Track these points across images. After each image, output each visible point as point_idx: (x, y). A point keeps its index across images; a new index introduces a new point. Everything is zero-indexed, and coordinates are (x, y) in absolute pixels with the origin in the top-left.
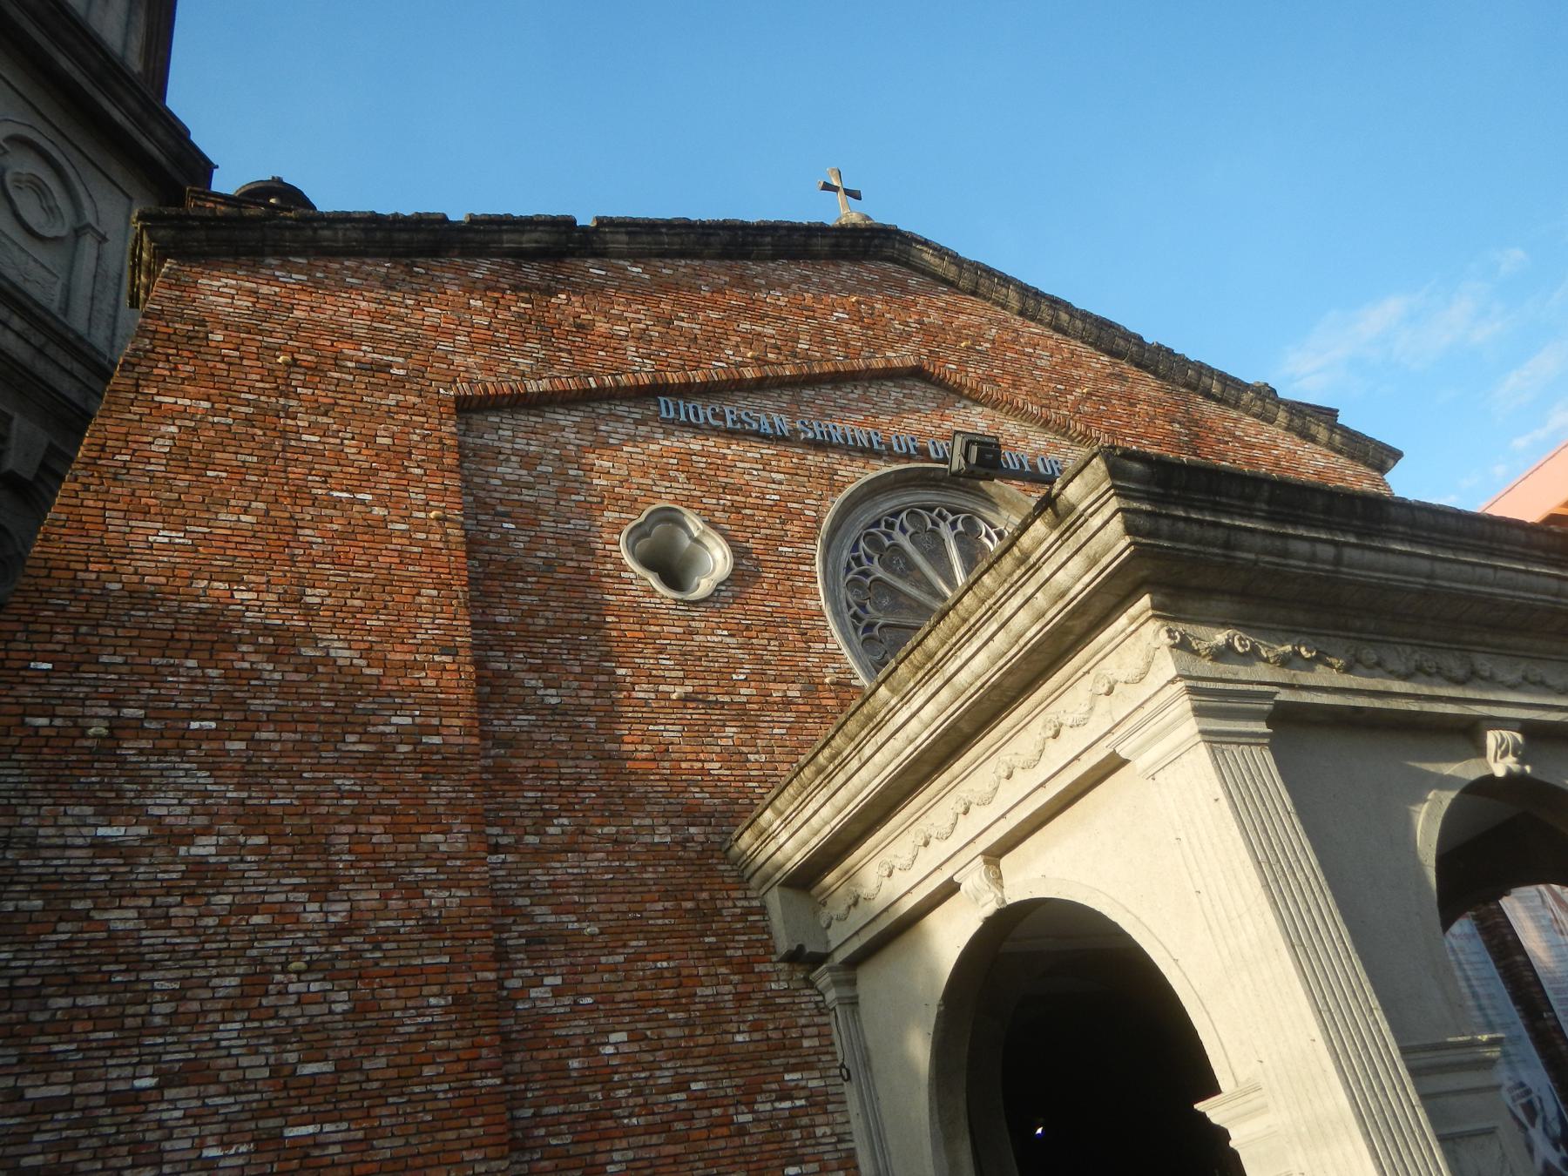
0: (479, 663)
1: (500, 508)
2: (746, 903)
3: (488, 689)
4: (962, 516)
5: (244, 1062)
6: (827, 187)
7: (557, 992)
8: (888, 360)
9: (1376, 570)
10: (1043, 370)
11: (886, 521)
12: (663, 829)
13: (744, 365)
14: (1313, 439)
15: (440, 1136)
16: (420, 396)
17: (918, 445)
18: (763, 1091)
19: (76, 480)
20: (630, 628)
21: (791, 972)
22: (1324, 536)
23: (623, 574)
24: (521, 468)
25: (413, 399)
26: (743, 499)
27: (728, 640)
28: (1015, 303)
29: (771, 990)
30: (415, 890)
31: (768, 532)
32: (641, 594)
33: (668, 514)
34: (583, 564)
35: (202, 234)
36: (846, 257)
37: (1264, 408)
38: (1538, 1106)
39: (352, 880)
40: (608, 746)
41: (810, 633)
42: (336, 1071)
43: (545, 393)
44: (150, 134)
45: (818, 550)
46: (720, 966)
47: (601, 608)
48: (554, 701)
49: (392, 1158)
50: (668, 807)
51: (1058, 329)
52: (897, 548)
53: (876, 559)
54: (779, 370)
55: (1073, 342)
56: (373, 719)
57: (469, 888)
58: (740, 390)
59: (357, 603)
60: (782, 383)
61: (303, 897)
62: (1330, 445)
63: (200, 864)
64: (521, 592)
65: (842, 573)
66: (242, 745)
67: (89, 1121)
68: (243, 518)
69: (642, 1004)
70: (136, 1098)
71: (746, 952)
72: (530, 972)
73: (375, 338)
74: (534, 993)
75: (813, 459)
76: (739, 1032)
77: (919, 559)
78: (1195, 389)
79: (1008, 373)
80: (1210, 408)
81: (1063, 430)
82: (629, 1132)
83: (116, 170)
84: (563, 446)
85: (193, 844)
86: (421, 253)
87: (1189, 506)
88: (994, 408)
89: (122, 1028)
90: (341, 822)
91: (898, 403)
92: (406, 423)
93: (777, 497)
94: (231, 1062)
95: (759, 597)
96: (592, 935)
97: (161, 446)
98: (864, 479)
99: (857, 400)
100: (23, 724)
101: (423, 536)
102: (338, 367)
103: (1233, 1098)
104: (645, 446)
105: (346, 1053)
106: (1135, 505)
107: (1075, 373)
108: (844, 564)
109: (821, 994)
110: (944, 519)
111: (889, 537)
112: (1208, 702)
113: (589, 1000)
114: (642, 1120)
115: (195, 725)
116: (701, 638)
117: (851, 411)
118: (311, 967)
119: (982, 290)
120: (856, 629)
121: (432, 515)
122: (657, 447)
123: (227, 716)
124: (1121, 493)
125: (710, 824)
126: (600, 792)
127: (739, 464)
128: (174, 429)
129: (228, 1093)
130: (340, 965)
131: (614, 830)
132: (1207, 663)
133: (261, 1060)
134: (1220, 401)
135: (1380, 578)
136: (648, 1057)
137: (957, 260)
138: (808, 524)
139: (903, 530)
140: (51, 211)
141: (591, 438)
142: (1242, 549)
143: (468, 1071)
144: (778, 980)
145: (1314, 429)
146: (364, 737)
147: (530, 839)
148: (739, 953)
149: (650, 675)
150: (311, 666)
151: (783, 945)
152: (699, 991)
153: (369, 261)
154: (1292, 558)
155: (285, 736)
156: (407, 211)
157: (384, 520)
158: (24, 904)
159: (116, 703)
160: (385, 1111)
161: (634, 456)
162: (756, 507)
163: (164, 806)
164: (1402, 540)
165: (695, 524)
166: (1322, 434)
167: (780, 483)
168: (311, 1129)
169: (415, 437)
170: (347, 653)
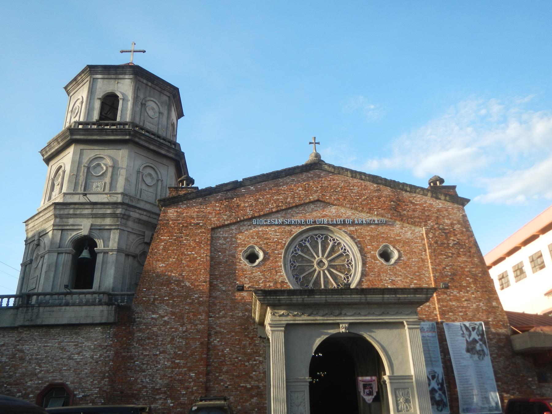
0: (211, 283)
1: (218, 250)
3: (213, 288)
4: (324, 236)
5: (170, 351)
6: (310, 143)
7: (218, 342)
8: (310, 199)
10: (355, 193)
12: (241, 313)
13: (273, 208)
14: (440, 199)
15: (197, 363)
16: (205, 229)
19: (149, 256)
20: (240, 273)
21: (260, 340)
22: (299, 297)
24: (224, 240)
25: (203, 230)
26: (268, 241)
27: (260, 274)
28: (349, 175)
30: (196, 325)
31: (273, 248)
34: (233, 260)
35: (168, 202)
36: (304, 172)
37: (423, 192)
38: (437, 375)
39: (187, 324)
40: (233, 298)
41: (278, 271)
42: (183, 353)
43: (229, 223)
44: (170, 152)
45: (283, 251)
47: (236, 269)
48: (224, 289)
49: (190, 366)
51: (362, 180)
52: (306, 246)
54: (281, 208)
55: (366, 182)
56: (192, 296)
57: (204, 325)
59: (191, 274)
60: (283, 210)
61: (179, 326)
62: (445, 200)
63: (165, 321)
64: (221, 267)
65: (290, 254)
66: (171, 301)
67: (151, 358)
68: (174, 260)
69: (232, 344)
70: (157, 355)
72: (214, 338)
73: (198, 217)
74: (215, 342)
75: (288, 228)
77: (310, 248)
78: (402, 190)
80: (405, 195)
81: (356, 209)
82: (227, 365)
83: (165, 161)
84: (231, 234)
85: (164, 318)
86: (207, 195)
87: (270, 296)
88: (339, 206)
89: (155, 345)
90: (186, 314)
92: (201, 236)
93: (276, 239)
94: (169, 351)
96: (225, 333)
97: (161, 247)
98: (299, 231)
100: (142, 299)
101: (202, 259)
102: (191, 225)
105: (184, 350)
106: (260, 297)
107: (364, 192)
108: (291, 252)
109: (265, 344)
110: (319, 237)
112: (272, 325)
113: (223, 343)
114: (230, 363)
115: (165, 298)
118: (180, 337)
119: (341, 173)
120: (291, 267)
121: (205, 255)
123: (170, 296)
124: (258, 296)
126: (230, 307)
128: (163, 244)
129: (168, 355)
130: (184, 337)
131: (232, 313)
132: (278, 317)
133: (173, 351)
134: (410, 192)
136: (232, 353)
137: (334, 167)
139: (308, 241)
140: (152, 178)
142: (282, 301)
143: (202, 354)
145: (440, 197)
147: (217, 315)
151: (259, 336)
152: (243, 342)
153: (198, 199)
155: (178, 299)
156: (204, 188)
157: (196, 257)
158: (143, 327)
159: (155, 295)
160: (189, 359)
162: (272, 242)
163: (161, 312)
164: (319, 295)
165: (257, 249)
166: (443, 197)
167: (278, 235)
168: (178, 361)
169: (203, 239)
170: (188, 284)
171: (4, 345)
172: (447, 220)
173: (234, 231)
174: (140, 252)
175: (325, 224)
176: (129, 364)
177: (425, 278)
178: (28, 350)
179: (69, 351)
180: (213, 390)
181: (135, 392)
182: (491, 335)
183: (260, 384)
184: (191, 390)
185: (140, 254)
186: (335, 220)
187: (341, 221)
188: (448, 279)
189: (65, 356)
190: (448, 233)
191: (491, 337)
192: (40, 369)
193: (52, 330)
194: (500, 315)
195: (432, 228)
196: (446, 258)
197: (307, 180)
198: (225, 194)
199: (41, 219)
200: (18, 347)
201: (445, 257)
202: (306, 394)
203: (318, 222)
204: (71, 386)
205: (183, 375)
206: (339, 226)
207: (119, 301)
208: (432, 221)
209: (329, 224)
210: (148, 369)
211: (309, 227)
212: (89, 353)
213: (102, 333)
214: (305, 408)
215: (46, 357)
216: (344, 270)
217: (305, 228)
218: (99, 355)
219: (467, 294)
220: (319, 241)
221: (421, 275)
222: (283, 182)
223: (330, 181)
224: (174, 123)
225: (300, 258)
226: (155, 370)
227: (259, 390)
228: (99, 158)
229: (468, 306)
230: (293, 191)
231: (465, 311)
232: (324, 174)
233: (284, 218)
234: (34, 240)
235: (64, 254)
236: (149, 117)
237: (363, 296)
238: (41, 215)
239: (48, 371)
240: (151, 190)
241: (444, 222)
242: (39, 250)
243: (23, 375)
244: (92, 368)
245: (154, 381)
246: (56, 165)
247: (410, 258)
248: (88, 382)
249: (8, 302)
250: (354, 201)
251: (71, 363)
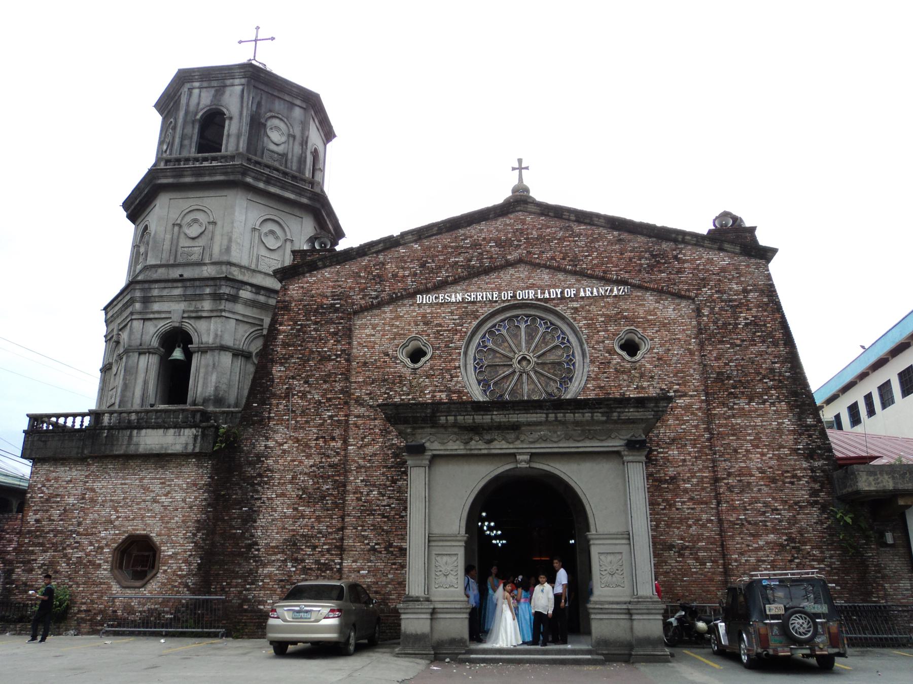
1: (364, 344)
5: (292, 493)
7: (362, 481)
13: (448, 276)
17: (512, 295)
25: (340, 314)
30: (328, 457)
45: (463, 343)
48: (371, 403)
55: (601, 229)
58: (449, 284)
61: (304, 458)
63: (284, 451)
67: (264, 503)
70: (272, 499)
81: (582, 274)
83: (297, 212)
84: (384, 319)
98: (490, 312)
99: (494, 278)
101: (339, 359)
111: (498, 330)
115: (284, 417)
117: (490, 283)
120: (475, 368)
122: (415, 314)
127: (443, 315)
128: (282, 336)
138: (463, 334)
139: (505, 327)
140: (277, 238)
146: (320, 419)
150: (309, 401)
155: (303, 419)
163: (278, 437)
167: (456, 320)
171: (71, 481)
172: (737, 284)
173: (388, 315)
174: (256, 349)
176: (234, 511)
177: (693, 381)
178: (101, 489)
179: (154, 491)
180: (353, 551)
181: (242, 550)
182: (799, 472)
184: (320, 550)
185: (257, 353)
186: (547, 291)
187: (557, 294)
188: (732, 382)
189: (148, 498)
190: (737, 306)
191: (798, 475)
192: (117, 515)
193: (130, 461)
194: (817, 438)
195: (710, 299)
196: (729, 348)
197: (504, 229)
198: (374, 257)
199: (120, 305)
200: (87, 484)
201: (729, 346)
202: (459, 558)
203: (519, 297)
204: (157, 540)
205: (310, 528)
206: (554, 302)
207: (221, 421)
208: (710, 287)
209: (537, 299)
210: (260, 519)
211: (505, 305)
212: (180, 495)
213: (197, 466)
215: (124, 498)
216: (561, 371)
217: (498, 307)
218: (193, 497)
219: (762, 406)
220: (523, 326)
221: (688, 376)
222: (464, 235)
223: (541, 229)
224: (316, 150)
226: (270, 520)
228: (196, 211)
229: (765, 425)
230: (480, 248)
231: (757, 434)
232: (532, 219)
233: (467, 291)
234: (112, 337)
235: (147, 354)
236: (273, 145)
237: (551, 411)
238: (119, 299)
239: (127, 518)
240: (274, 256)
241: (730, 289)
242: (119, 350)
243: (94, 522)
244: (183, 517)
245: (269, 536)
246: (142, 223)
247: (669, 350)
248: (179, 534)
249: (74, 422)
250: (579, 261)
251: (157, 508)
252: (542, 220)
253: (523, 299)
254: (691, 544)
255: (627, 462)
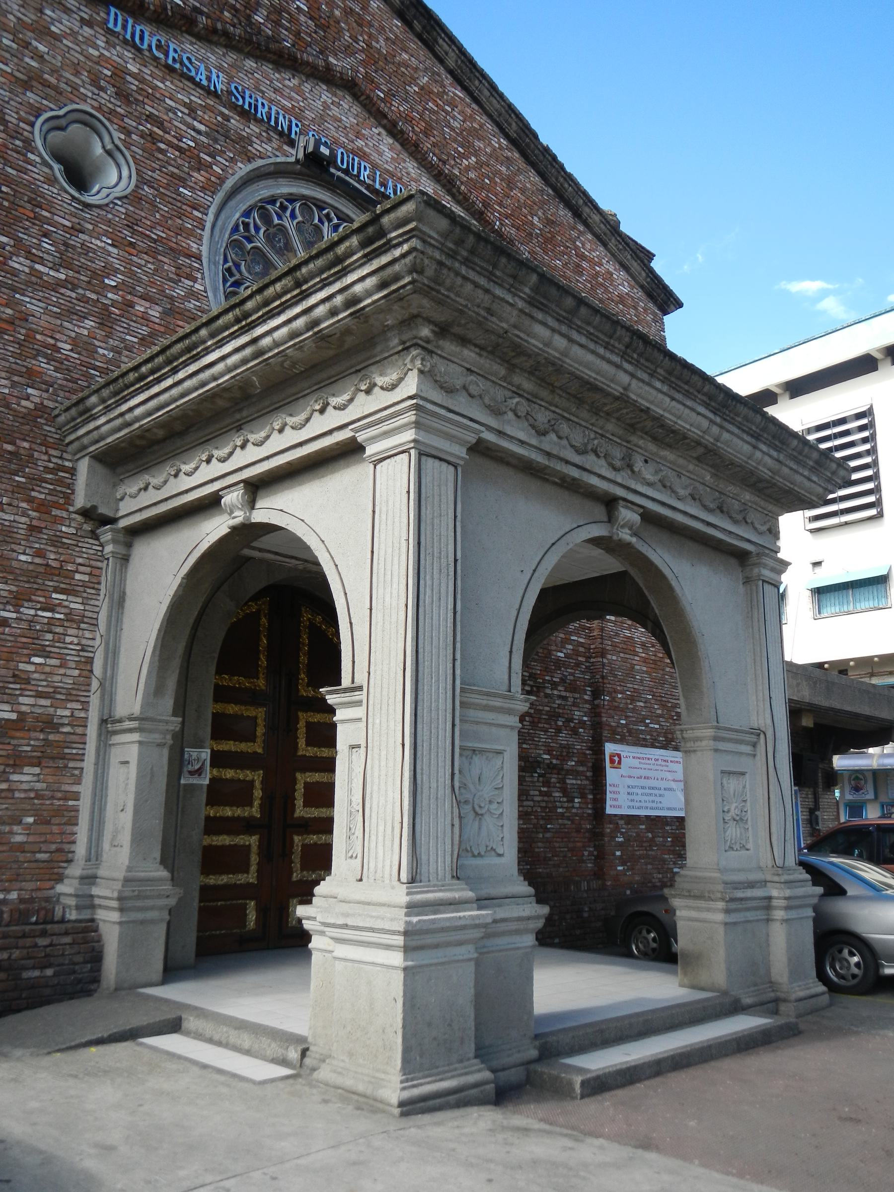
2: (60, 462)
9: (590, 369)
10: (452, 129)
11: (281, 203)
18: (30, 600)
23: (30, 155)
27: (110, 249)
29: (61, 531)
31: (176, 171)
32: (42, 179)
33: (87, 117)
46: (23, 501)
50: (14, 366)
52: (282, 229)
53: (262, 231)
55: (485, 117)
71: (49, 498)
76: (24, 553)
79: (424, 120)
91: (326, 106)
95: (149, 223)
99: (291, 89)
103: (346, 690)
104: (84, 47)
109: (102, 545)
111: (280, 217)
116: (86, 237)
117: (282, 96)
120: (225, 281)
122: (96, 53)
125: (47, 391)
127: (168, 101)
135: (590, 376)
138: (213, 179)
139: (293, 216)
141: (34, 17)
144: (69, 526)
148: (43, 496)
149: (30, 252)
154: (533, 338)
161: (72, 52)
175: (359, 181)
183: (60, 712)
214: (502, 826)
223: (394, 43)
225: (259, 263)
227: (51, 737)
250: (449, 155)
252: (397, 26)
253: (346, 172)
254: (558, 762)
255: (764, 581)
